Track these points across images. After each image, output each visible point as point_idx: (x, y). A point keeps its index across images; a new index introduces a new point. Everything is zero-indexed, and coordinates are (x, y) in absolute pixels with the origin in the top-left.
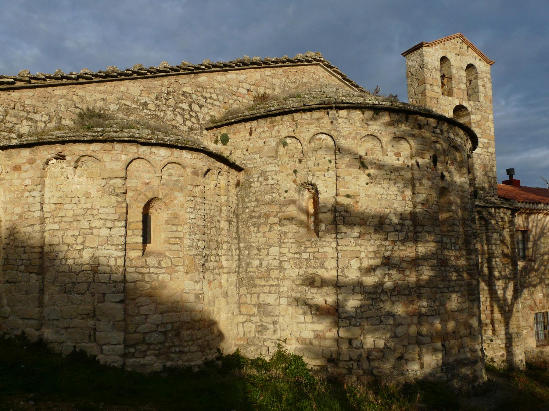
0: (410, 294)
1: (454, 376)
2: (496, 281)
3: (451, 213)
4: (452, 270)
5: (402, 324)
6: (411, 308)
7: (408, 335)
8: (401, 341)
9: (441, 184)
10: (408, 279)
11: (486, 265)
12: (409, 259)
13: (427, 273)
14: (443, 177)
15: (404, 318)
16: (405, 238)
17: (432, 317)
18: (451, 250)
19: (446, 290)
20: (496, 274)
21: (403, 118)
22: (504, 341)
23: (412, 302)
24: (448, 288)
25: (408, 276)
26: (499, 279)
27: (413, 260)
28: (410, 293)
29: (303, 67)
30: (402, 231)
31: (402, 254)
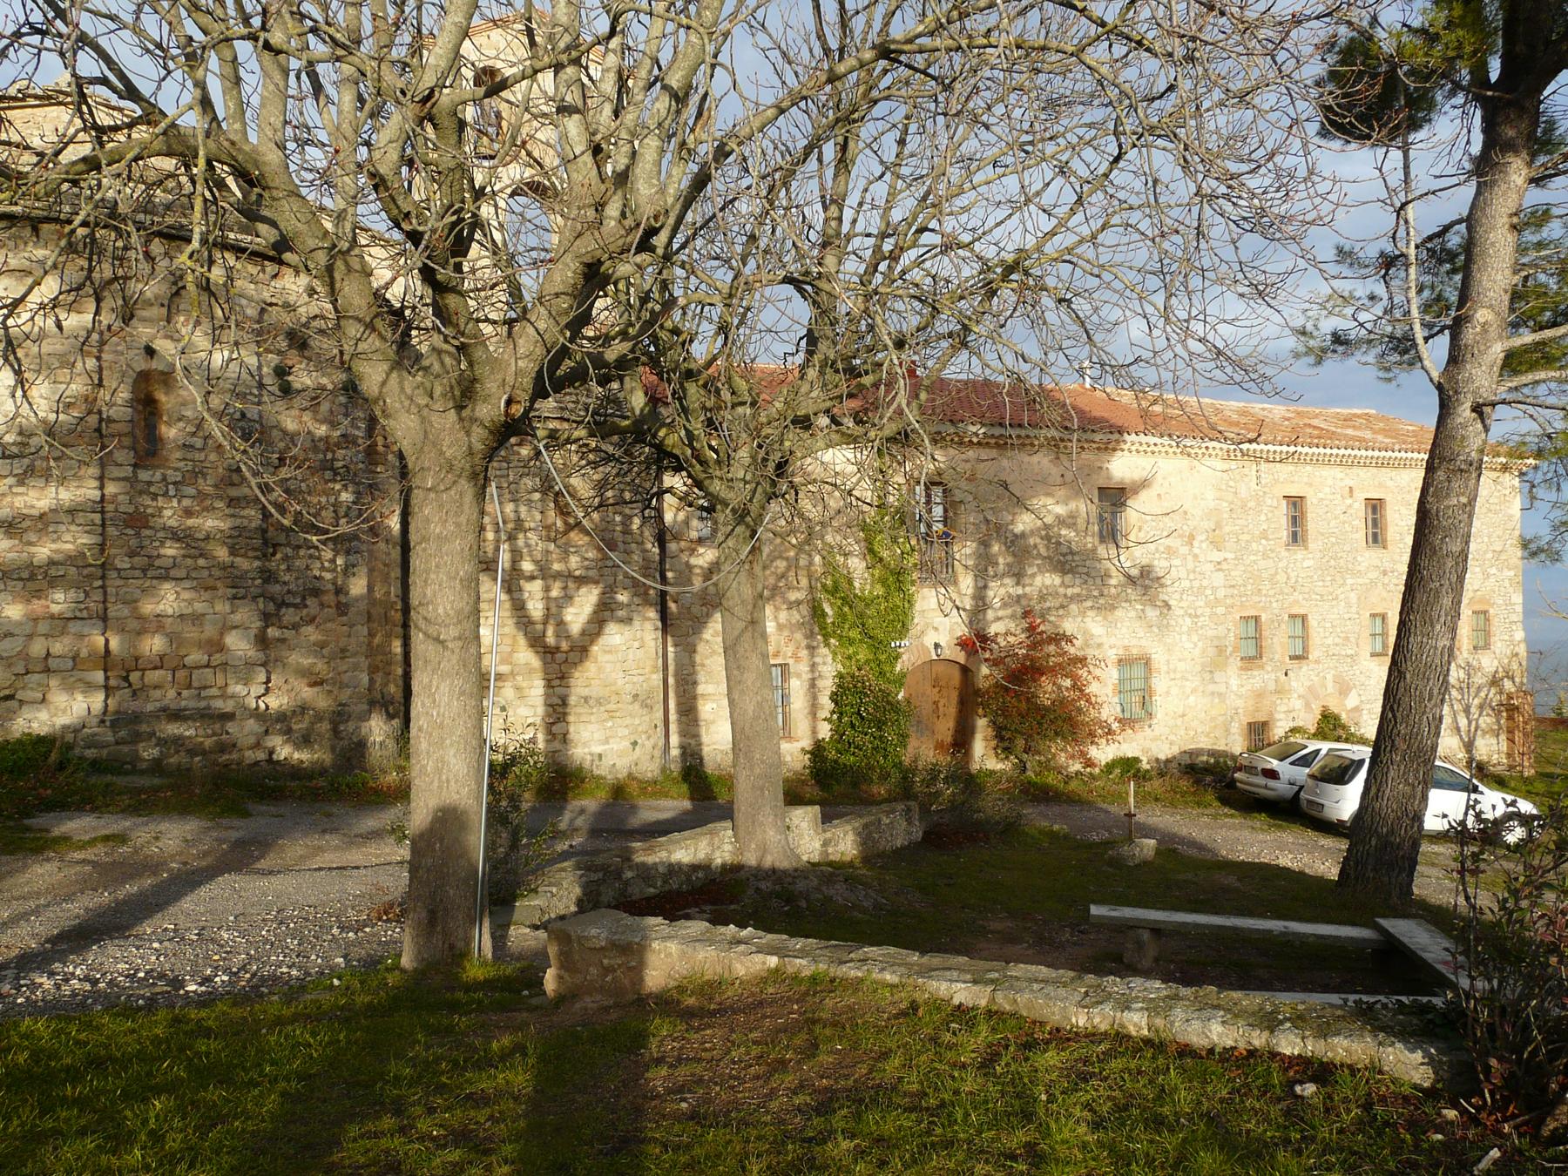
0: (32, 577)
1: (137, 737)
2: (522, 582)
3: (181, 424)
4: (161, 534)
5: (12, 635)
6: (37, 606)
7: (24, 656)
8: (9, 666)
9: (141, 364)
10: (33, 549)
11: (506, 546)
12: (35, 512)
13: (73, 540)
14: (150, 352)
15: (19, 624)
16: (25, 472)
17: (79, 623)
18: (165, 494)
19: (137, 573)
20: (527, 566)
21: (27, 232)
22: (541, 710)
23: (38, 594)
24: (144, 571)
25: (30, 544)
26: (532, 578)
27: (42, 516)
28: (32, 577)
29: (29, 110)
30: (20, 456)
31: (19, 502)
